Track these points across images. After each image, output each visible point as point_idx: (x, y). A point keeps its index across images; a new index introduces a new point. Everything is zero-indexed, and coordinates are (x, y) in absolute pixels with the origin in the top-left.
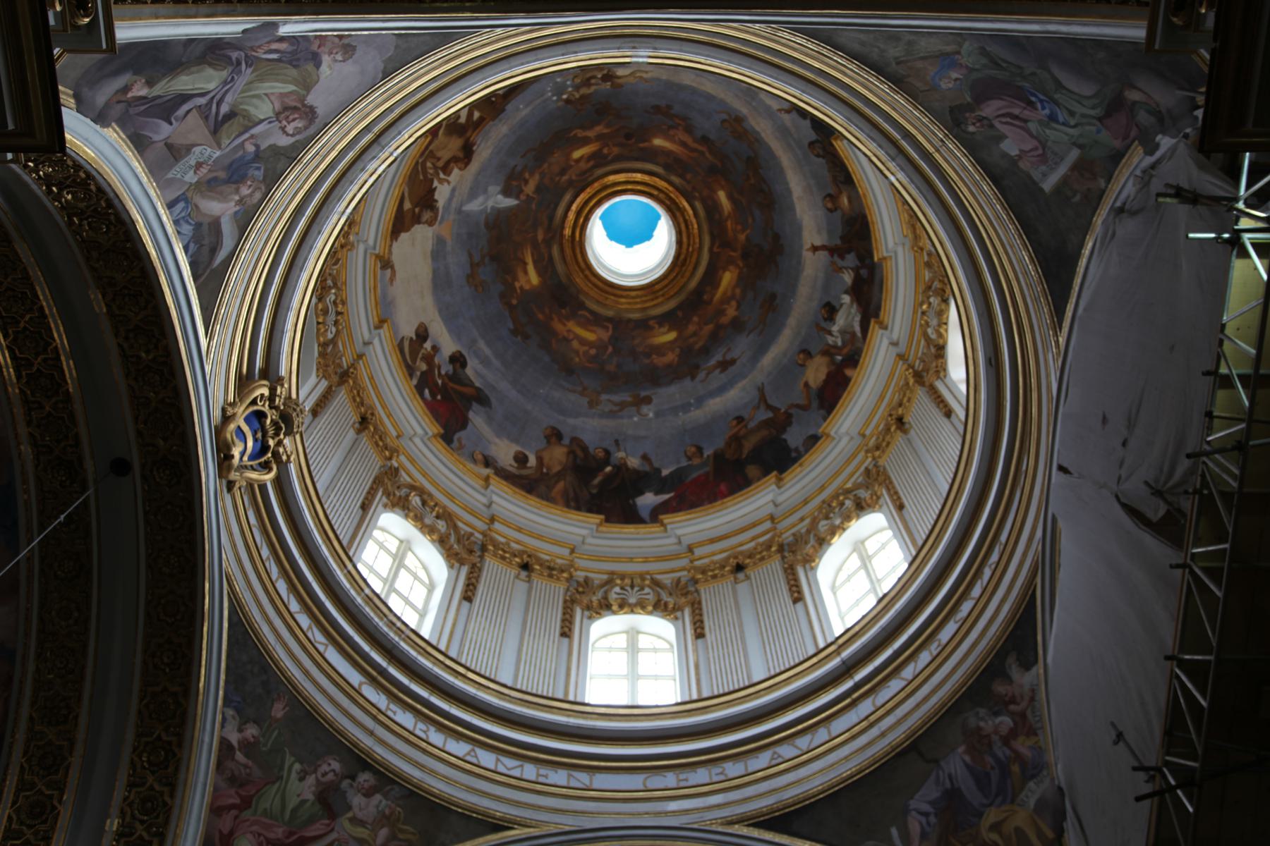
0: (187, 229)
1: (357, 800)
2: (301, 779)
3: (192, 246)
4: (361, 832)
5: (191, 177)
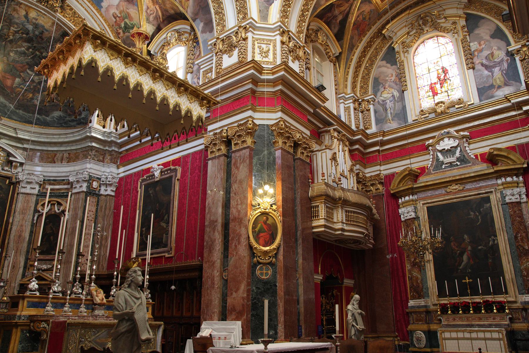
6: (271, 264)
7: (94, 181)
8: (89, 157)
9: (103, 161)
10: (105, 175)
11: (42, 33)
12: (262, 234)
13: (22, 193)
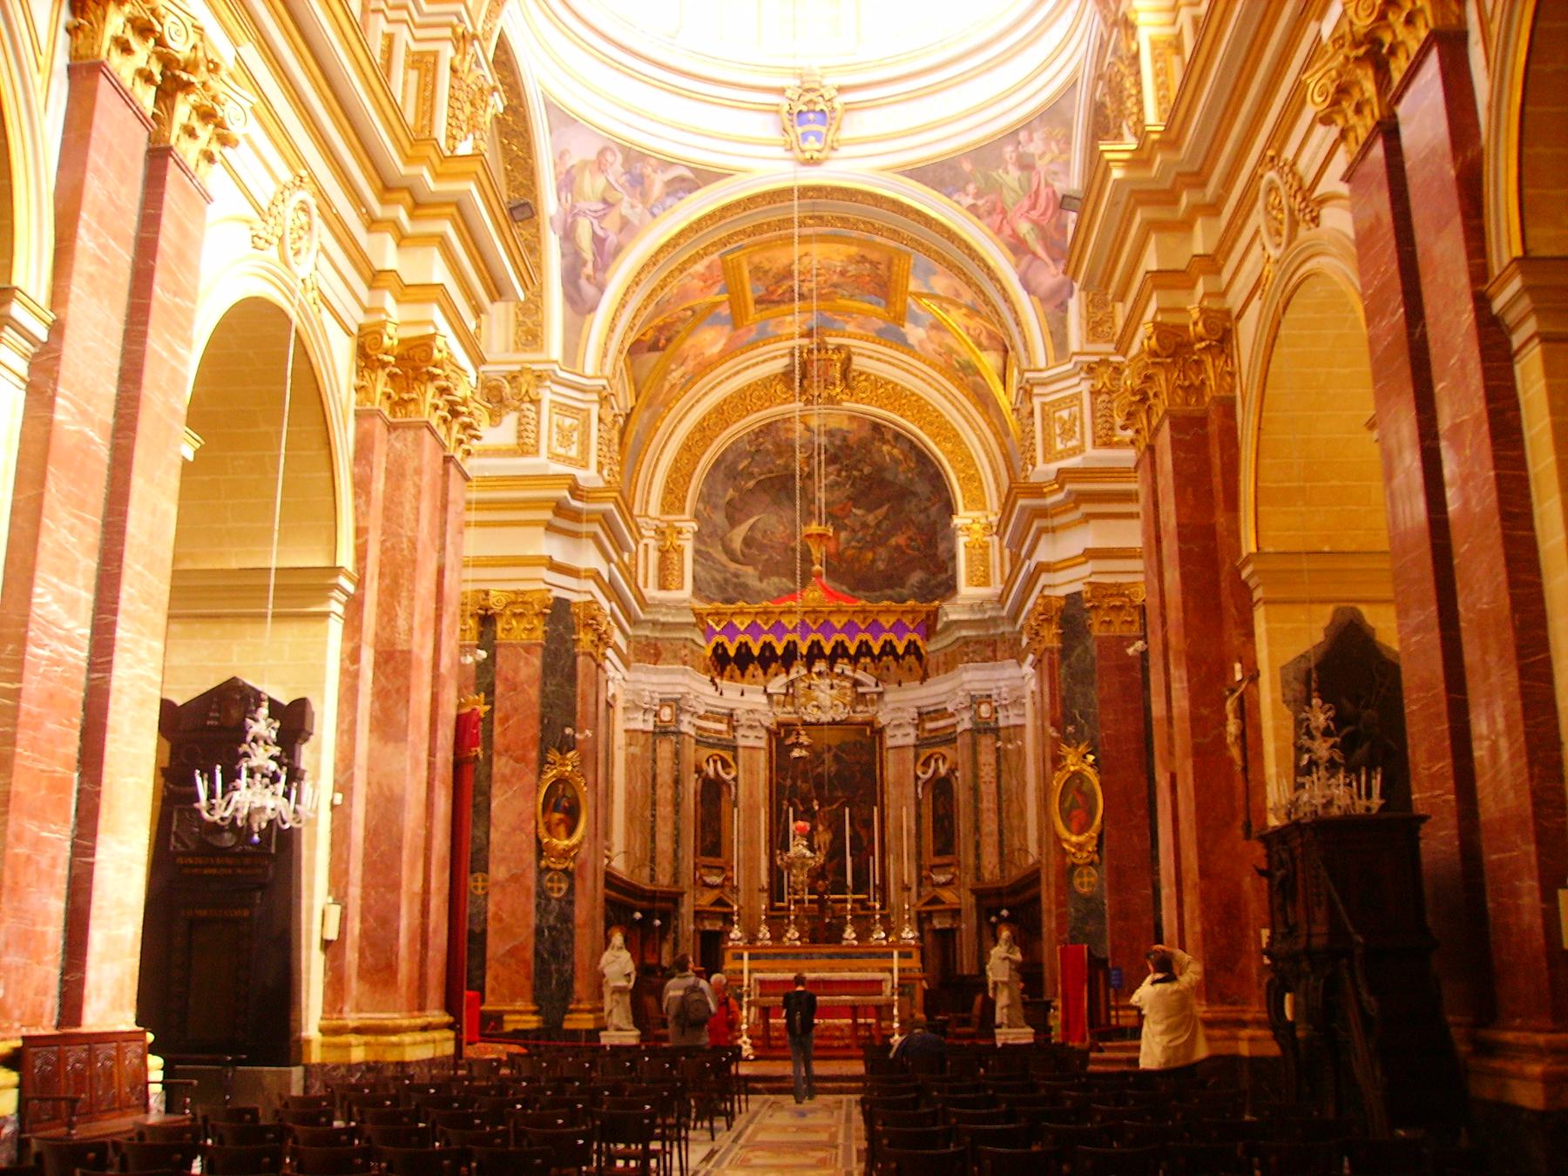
0: (669, 201)
1: (1035, 147)
2: (1007, 173)
3: (680, 194)
4: (1048, 157)
5: (639, 209)
6: (1092, 863)
7: (980, 703)
8: (966, 659)
9: (994, 659)
10: (998, 688)
11: (845, 439)
12: (1074, 813)
13: (892, 748)
